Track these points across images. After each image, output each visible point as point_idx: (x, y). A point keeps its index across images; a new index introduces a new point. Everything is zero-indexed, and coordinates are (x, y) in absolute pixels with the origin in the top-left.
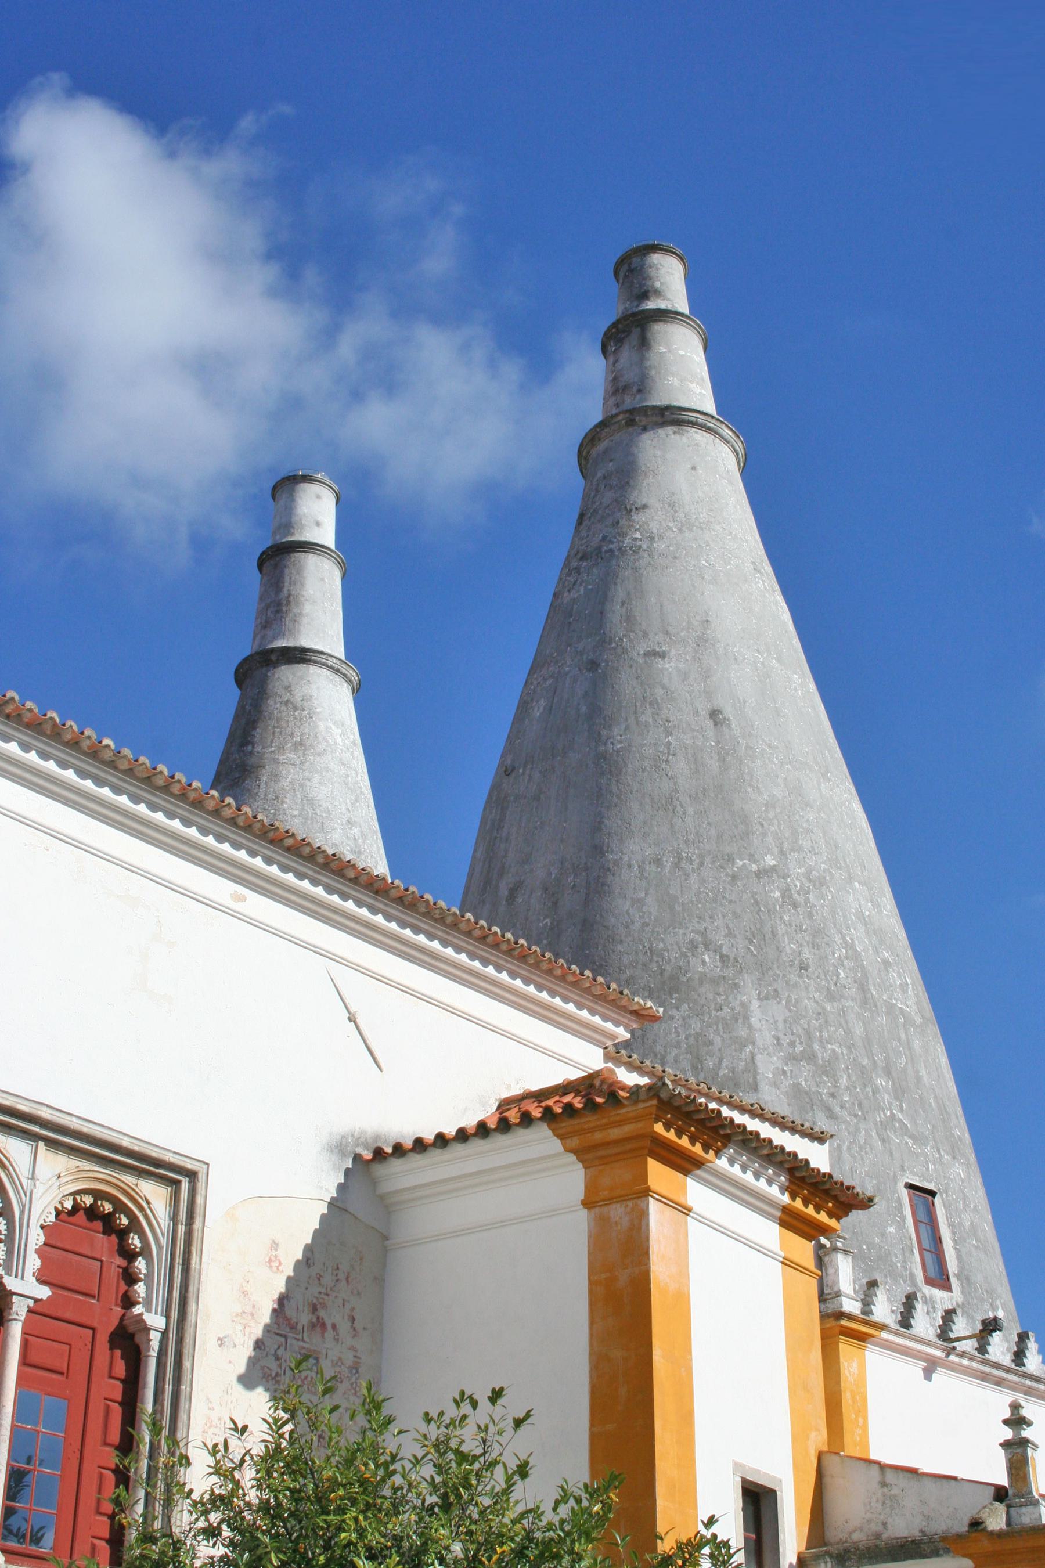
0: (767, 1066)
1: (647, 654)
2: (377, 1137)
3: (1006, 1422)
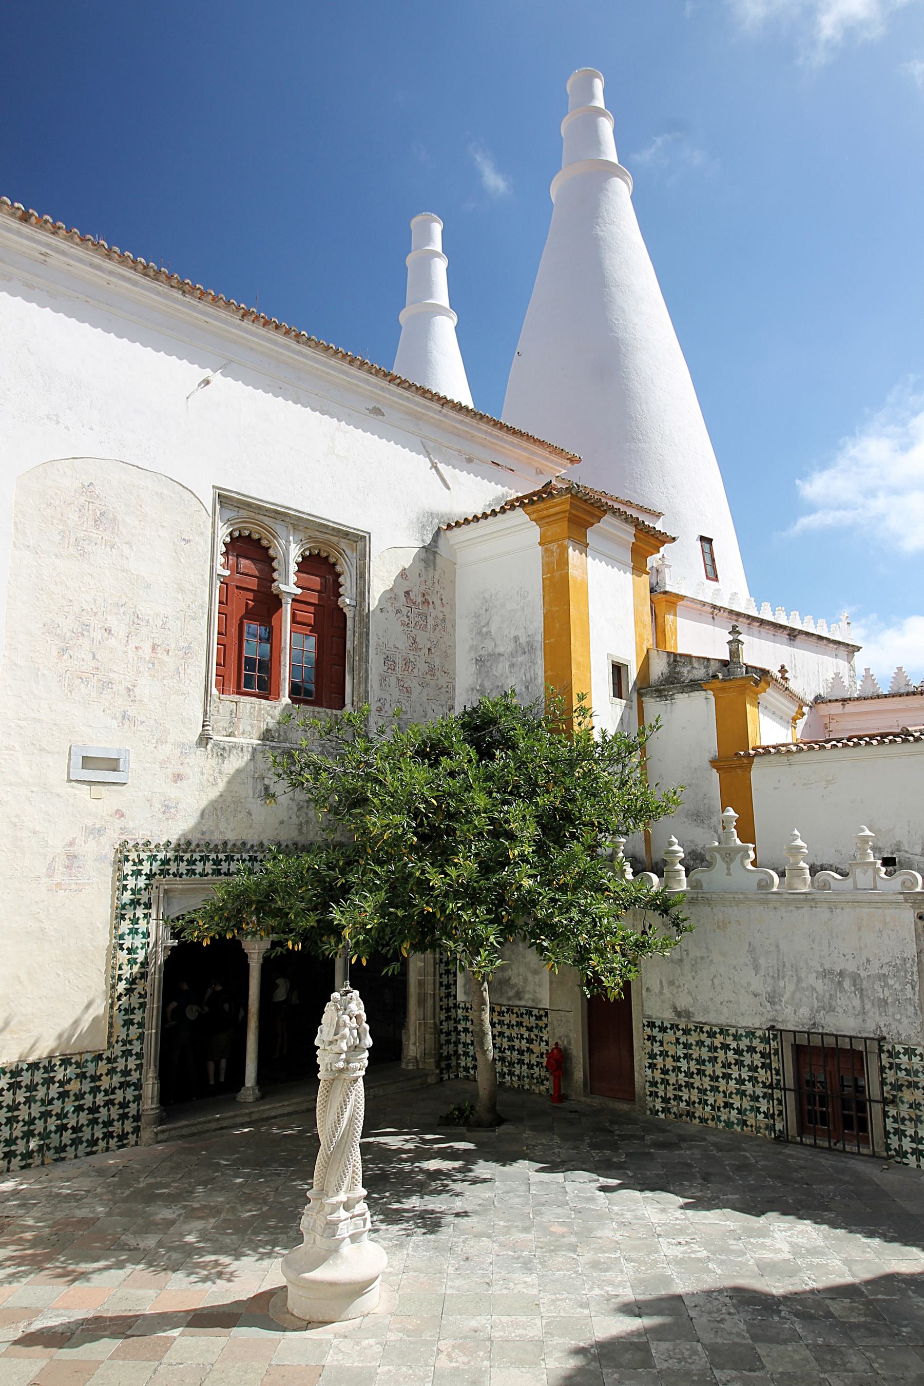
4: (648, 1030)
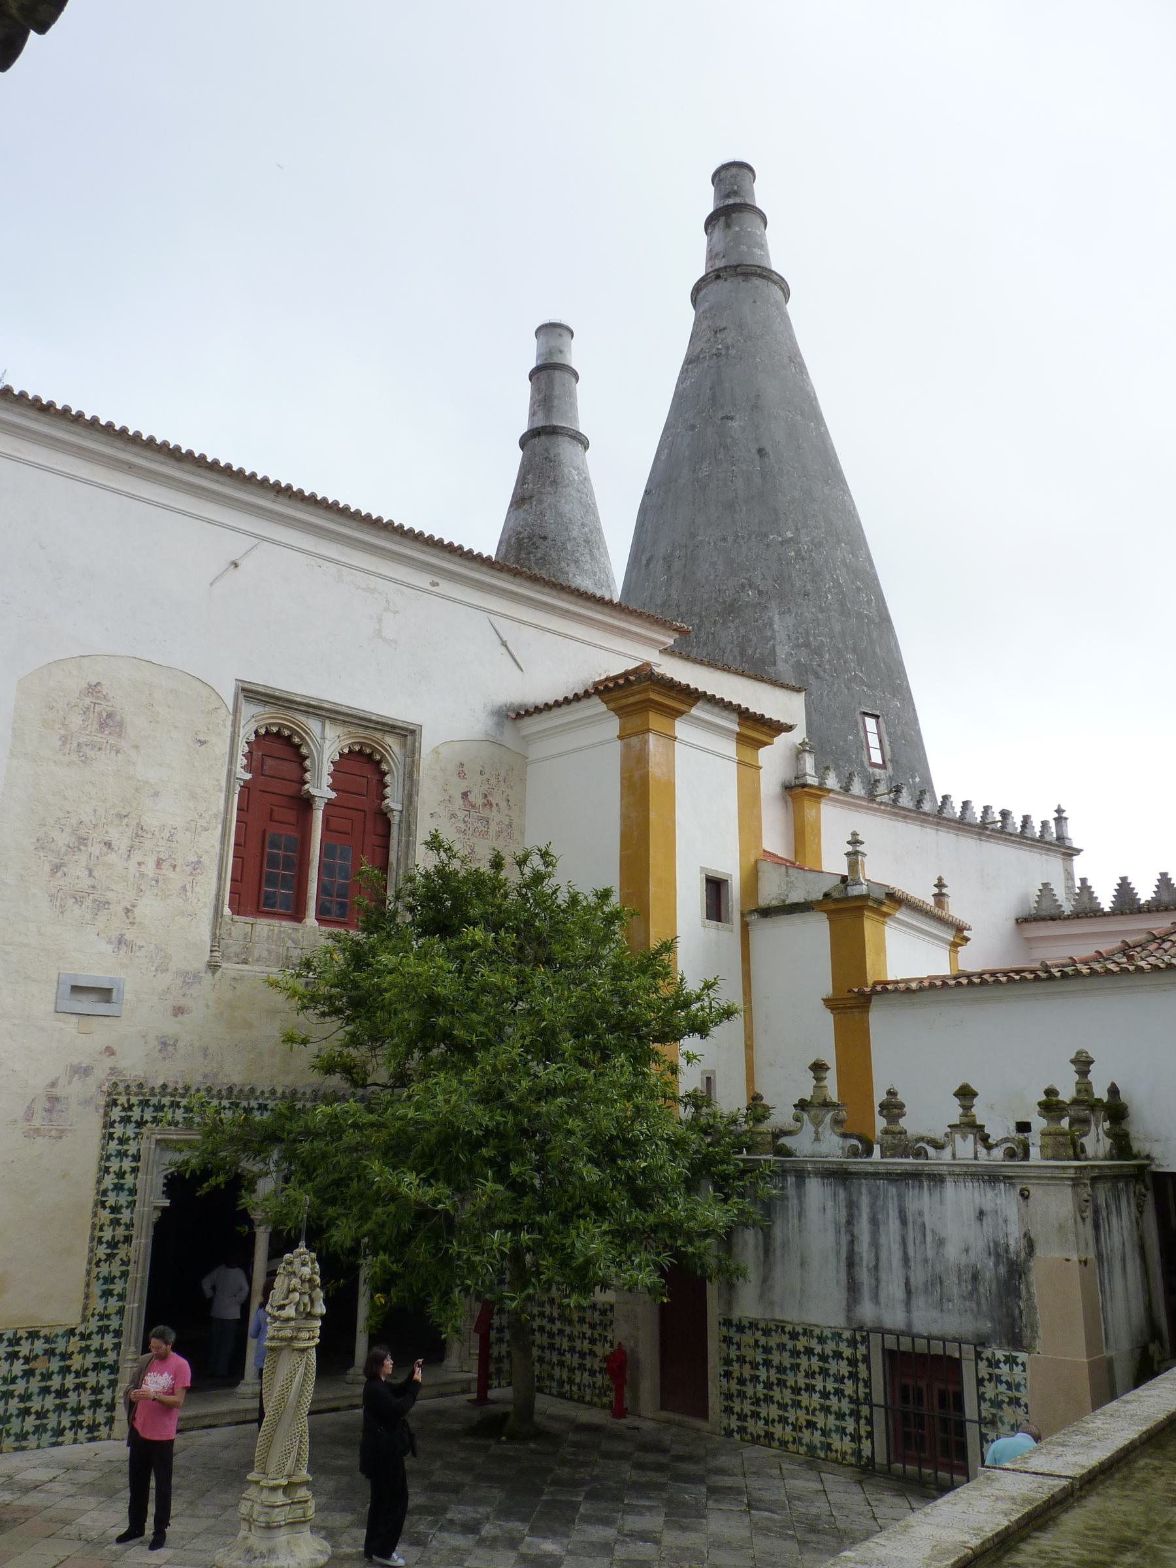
0: (782, 651)
1: (722, 418)
2: (520, 706)
3: (848, 843)
4: (724, 1329)
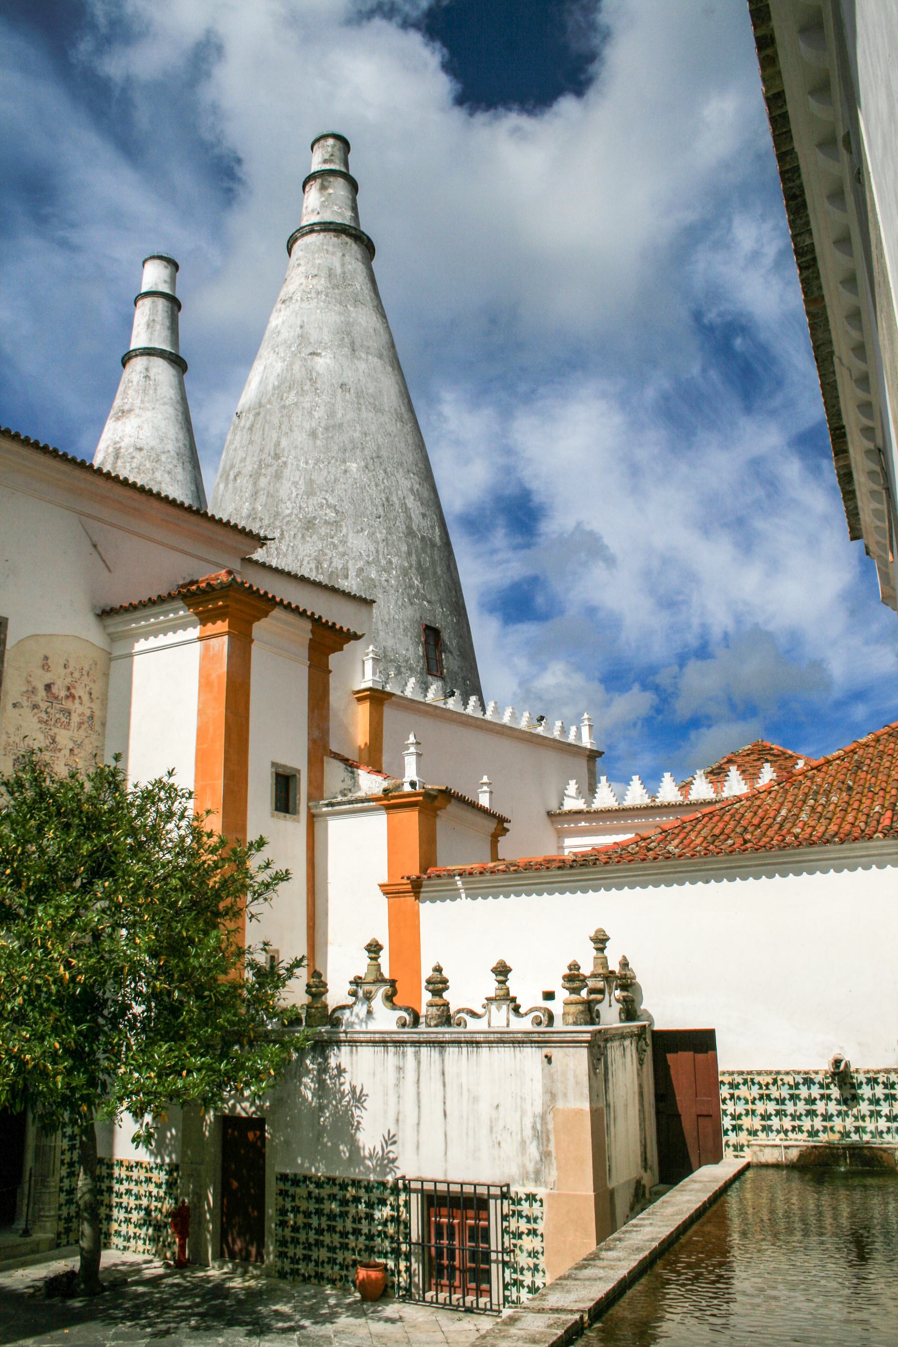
1: (311, 354)
4: (281, 1185)
